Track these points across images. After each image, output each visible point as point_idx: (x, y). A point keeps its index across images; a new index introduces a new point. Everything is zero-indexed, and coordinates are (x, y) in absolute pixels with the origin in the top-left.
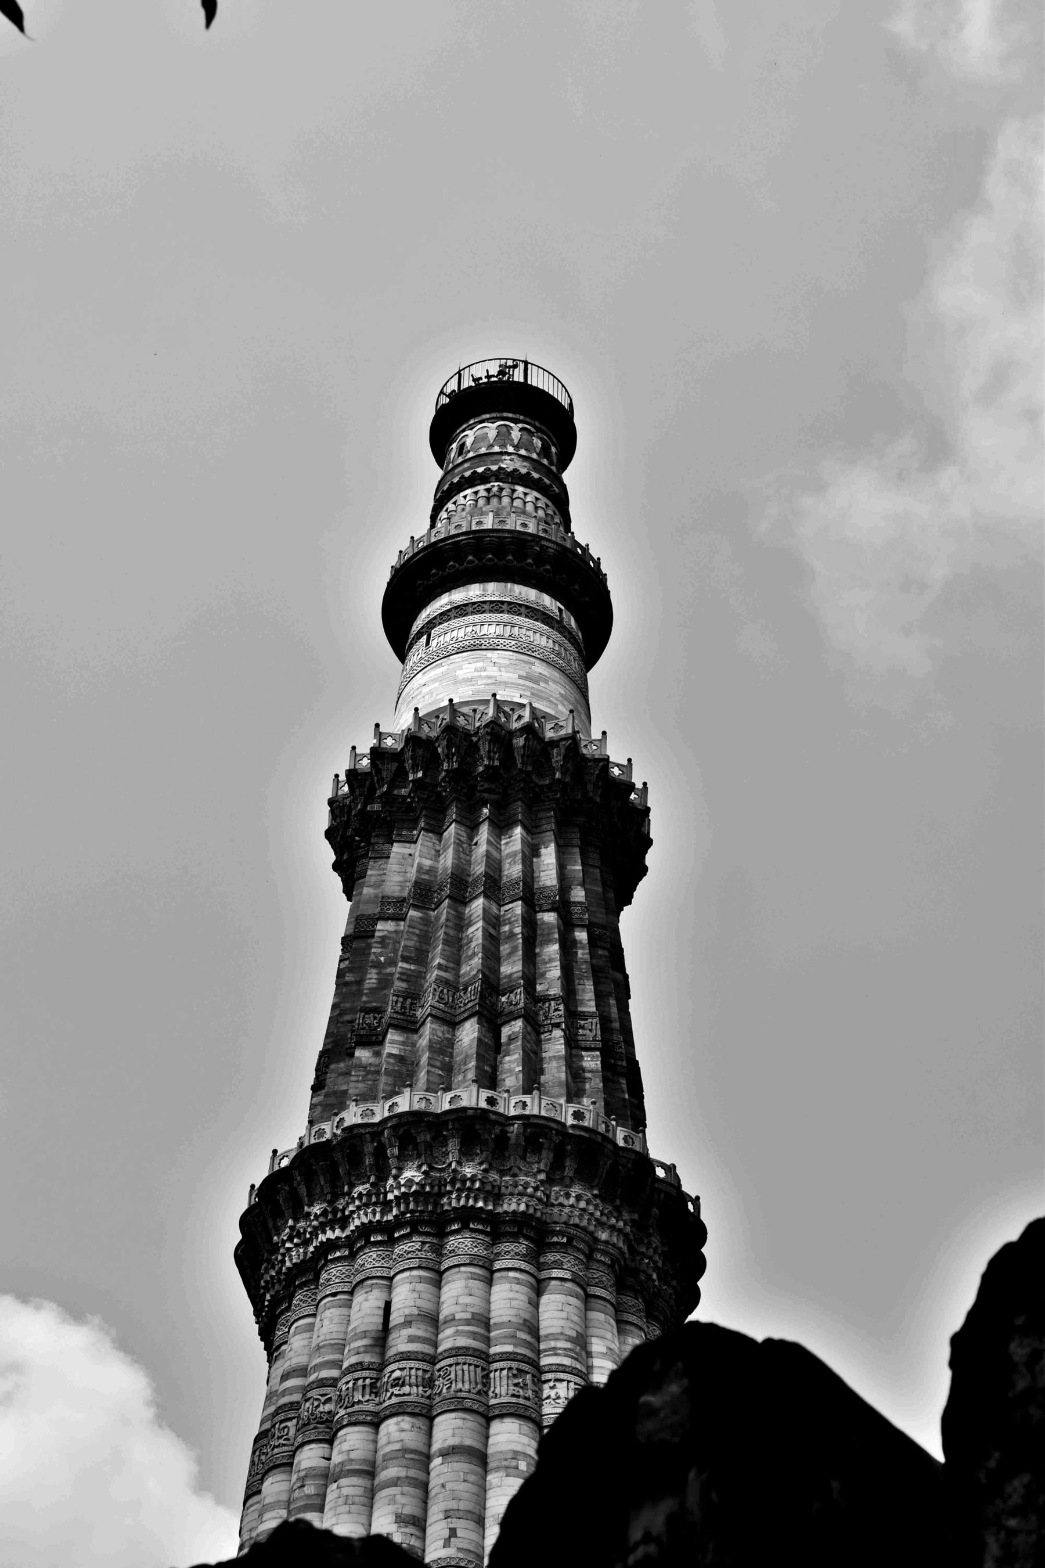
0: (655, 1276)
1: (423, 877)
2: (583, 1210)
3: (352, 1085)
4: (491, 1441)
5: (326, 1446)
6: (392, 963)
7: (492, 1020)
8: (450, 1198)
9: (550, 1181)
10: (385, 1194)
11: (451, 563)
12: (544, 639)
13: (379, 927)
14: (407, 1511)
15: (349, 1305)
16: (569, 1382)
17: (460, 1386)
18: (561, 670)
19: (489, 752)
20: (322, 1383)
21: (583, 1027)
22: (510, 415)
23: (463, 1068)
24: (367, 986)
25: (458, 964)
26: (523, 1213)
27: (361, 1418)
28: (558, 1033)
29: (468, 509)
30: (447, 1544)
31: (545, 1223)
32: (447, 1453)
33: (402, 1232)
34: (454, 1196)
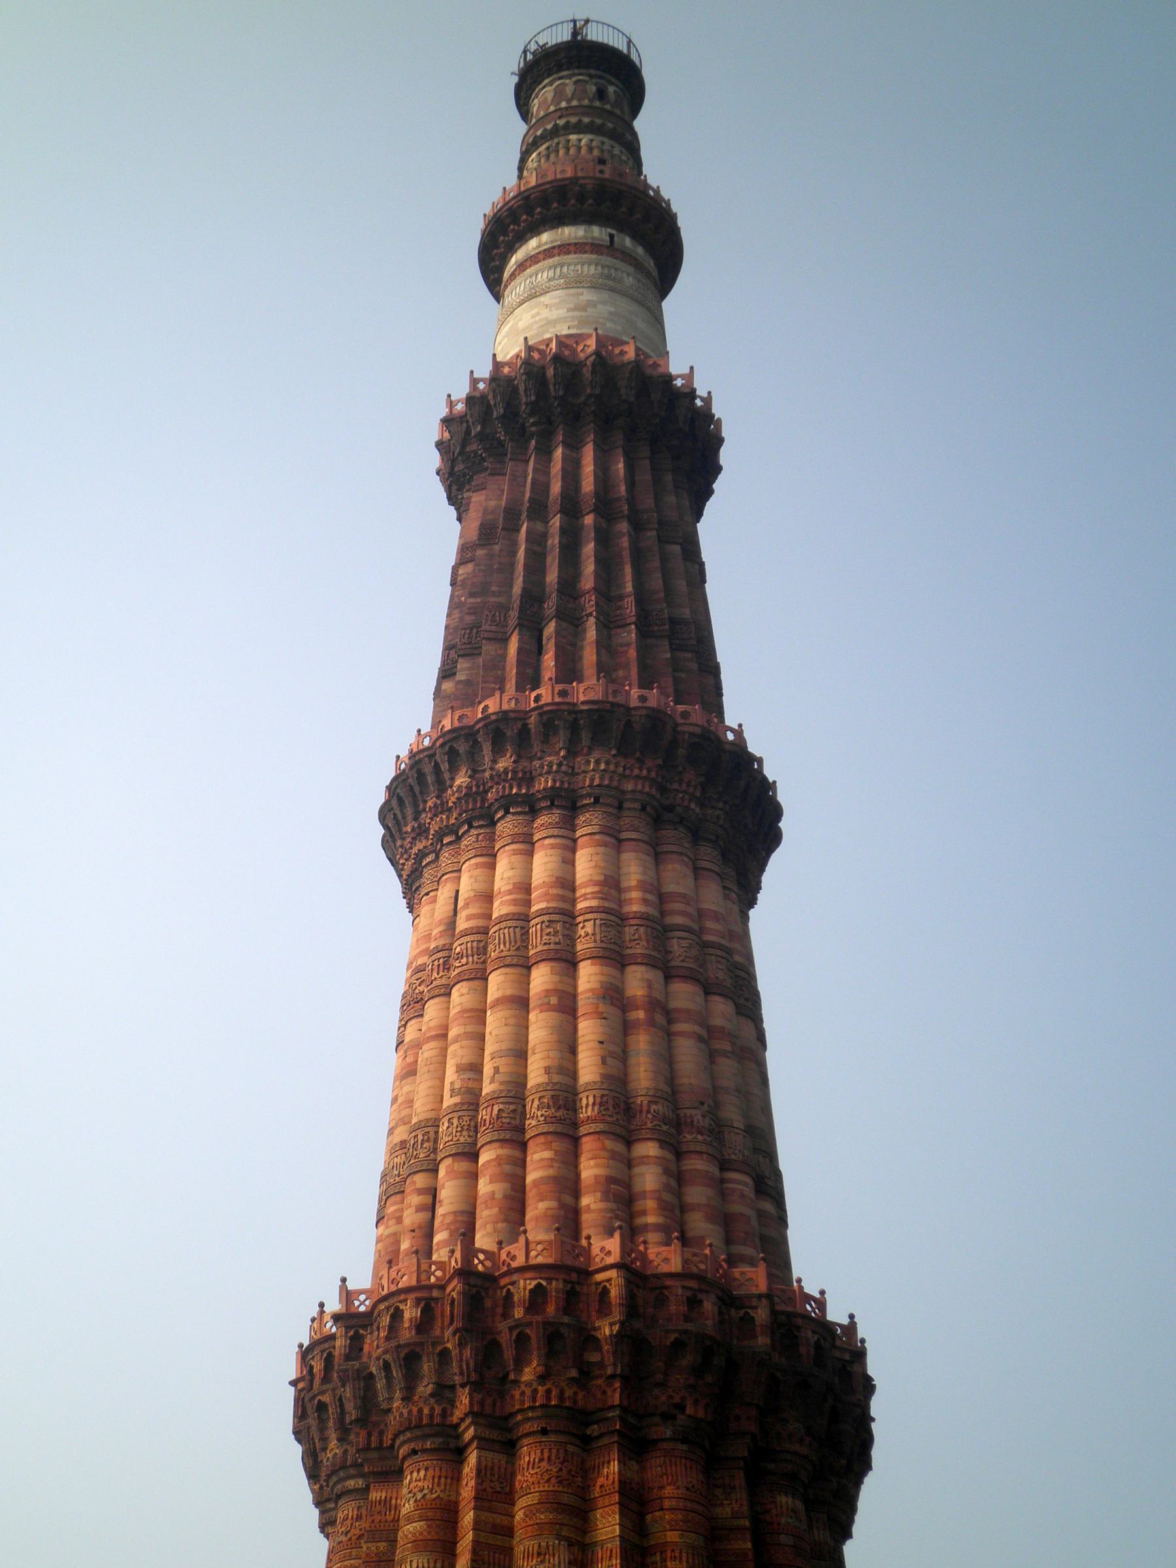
0: (693, 806)
1: (491, 517)
9: (572, 753)
15: (434, 900)
19: (526, 391)
28: (592, 620)
31: (574, 791)
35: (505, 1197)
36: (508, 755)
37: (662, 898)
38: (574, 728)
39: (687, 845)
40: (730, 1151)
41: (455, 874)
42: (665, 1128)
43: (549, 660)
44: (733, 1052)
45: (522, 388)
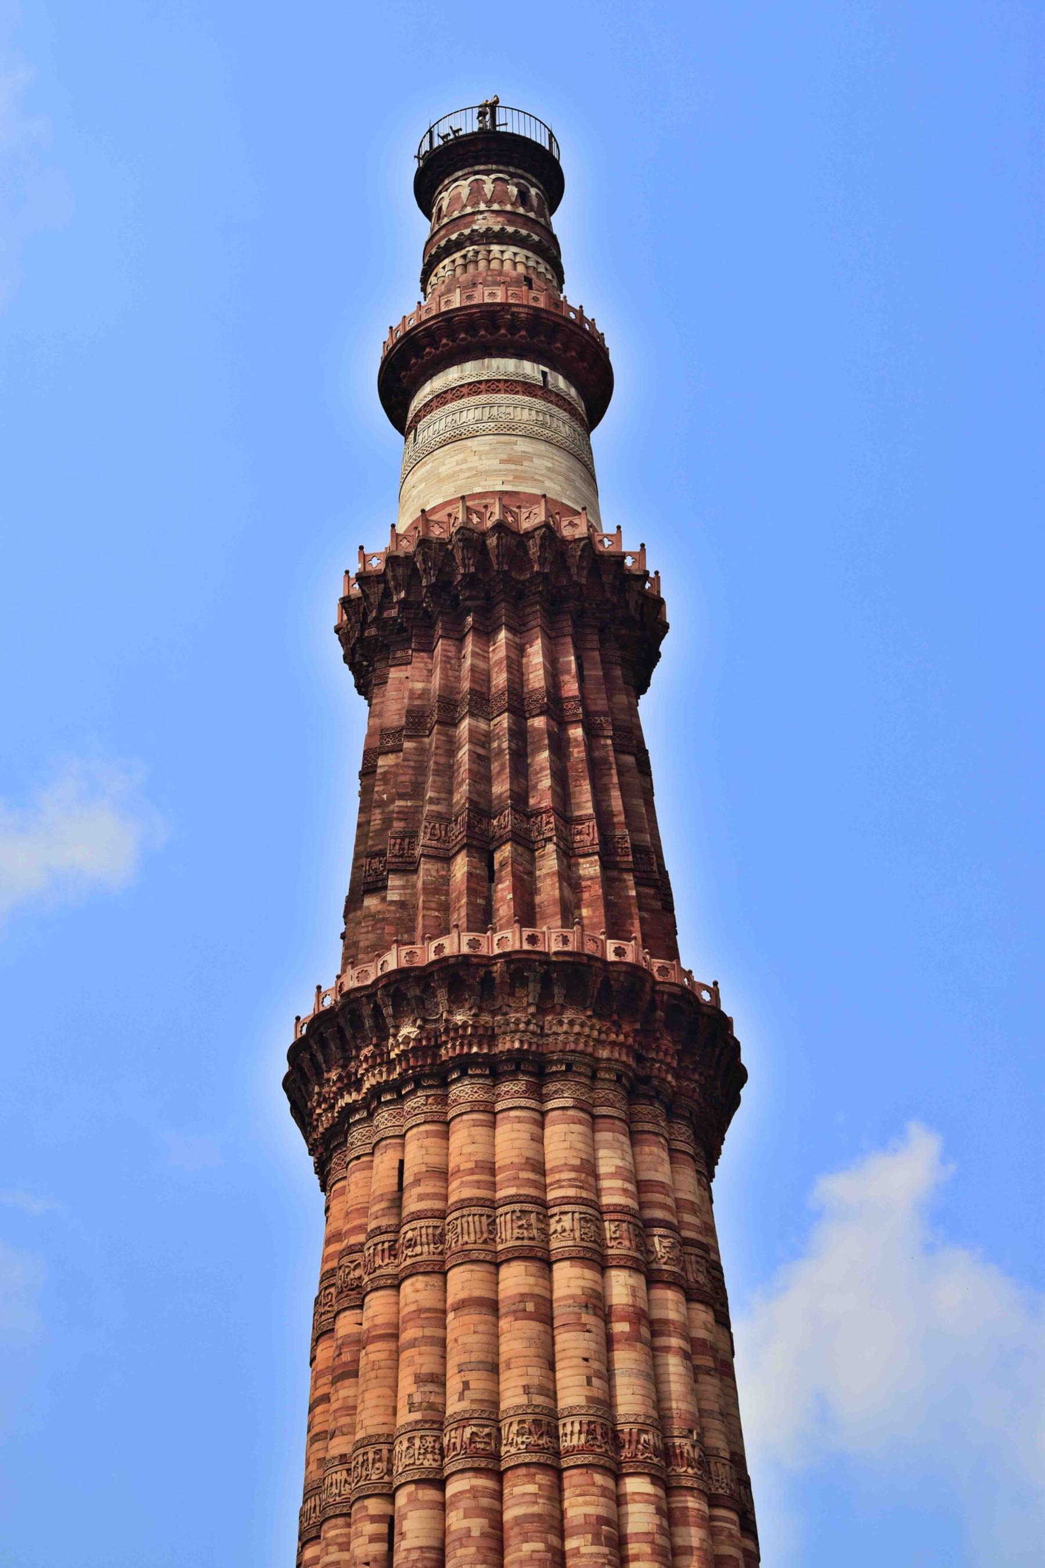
0: (669, 1078)
1: (416, 702)
2: (576, 1034)
3: (362, 937)
4: (501, 1287)
5: (358, 1311)
6: (392, 800)
7: (482, 848)
8: (446, 1048)
9: (542, 1010)
10: (389, 1053)
11: (428, 350)
12: (526, 411)
13: (380, 763)
14: (425, 1370)
15: (370, 1166)
16: (573, 1213)
17: (466, 1238)
18: (548, 441)
19: (463, 559)
20: (351, 1250)
21: (580, 833)
22: (482, 167)
23: (458, 906)
24: (372, 829)
25: (451, 792)
26: (518, 1050)
27: (382, 1283)
28: (551, 847)
29: (447, 281)
30: (461, 1398)
31: (543, 1054)
32: (461, 1306)
33: (408, 1089)
34: (449, 1046)
35: (483, 1535)
36: (467, 1006)
37: (641, 1186)
38: (546, 983)
39: (663, 1124)
40: (717, 1485)
41: (398, 1141)
42: (656, 1460)
43: (504, 890)
44: (716, 1369)
45: (458, 555)
